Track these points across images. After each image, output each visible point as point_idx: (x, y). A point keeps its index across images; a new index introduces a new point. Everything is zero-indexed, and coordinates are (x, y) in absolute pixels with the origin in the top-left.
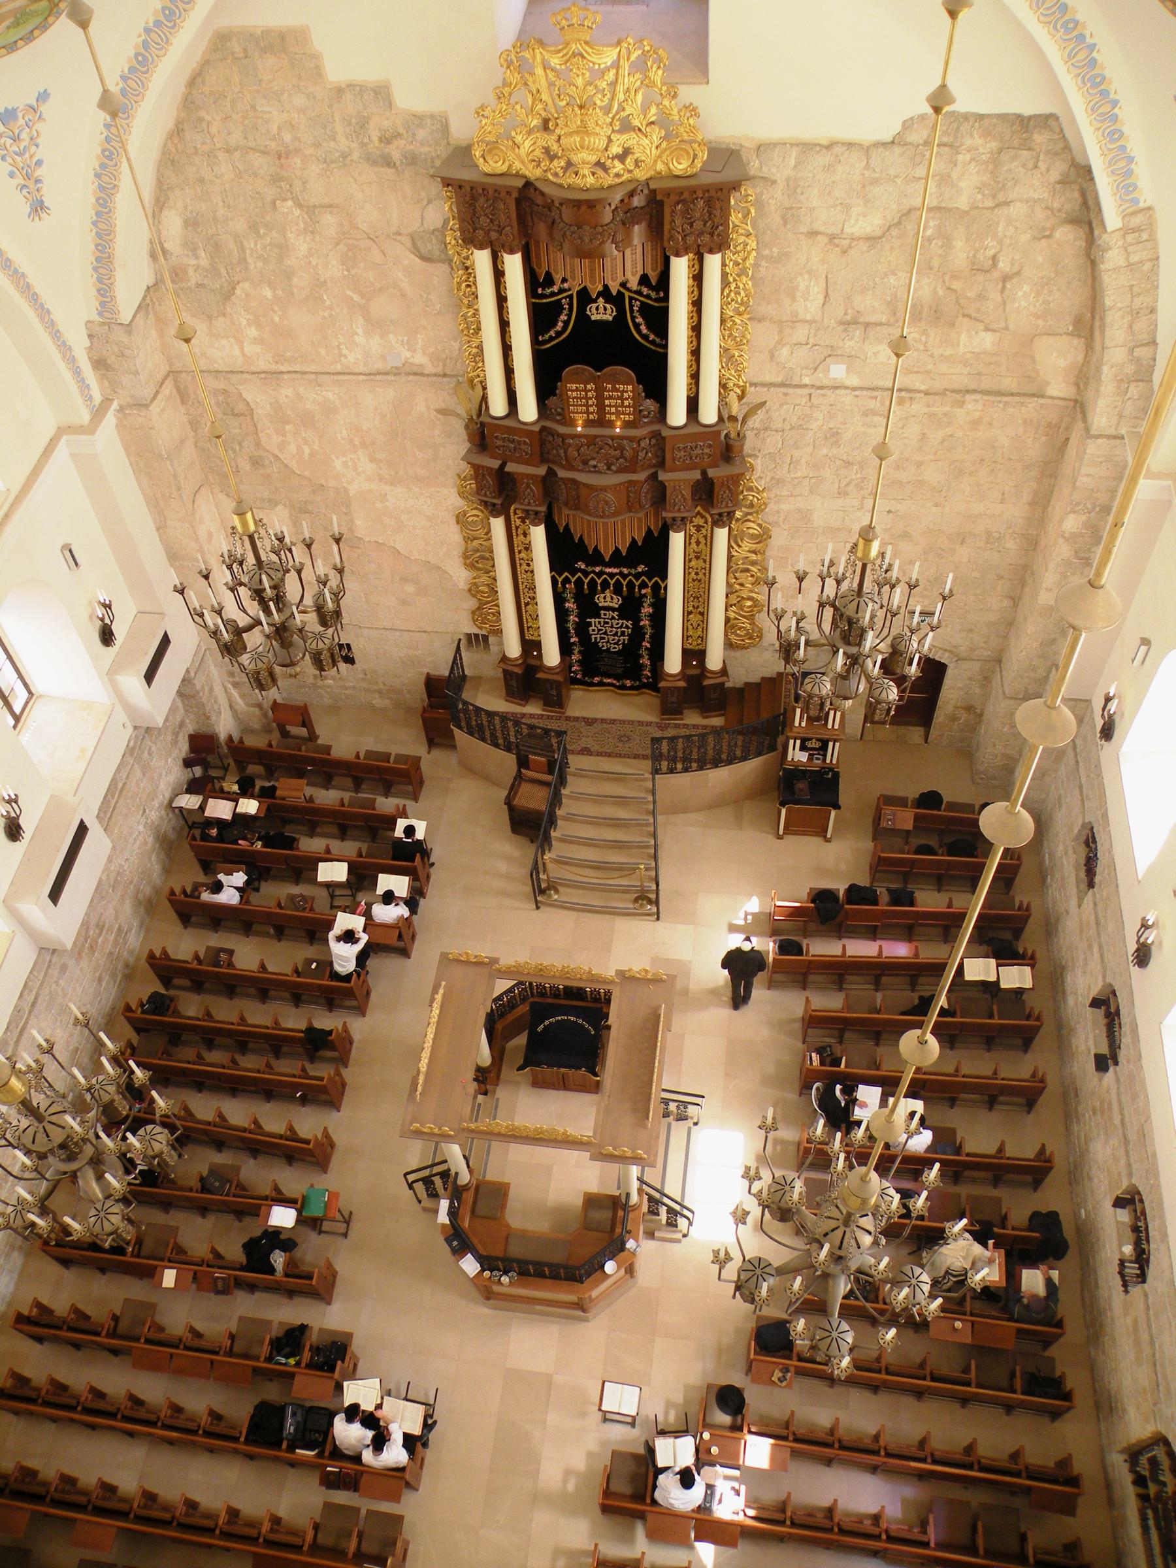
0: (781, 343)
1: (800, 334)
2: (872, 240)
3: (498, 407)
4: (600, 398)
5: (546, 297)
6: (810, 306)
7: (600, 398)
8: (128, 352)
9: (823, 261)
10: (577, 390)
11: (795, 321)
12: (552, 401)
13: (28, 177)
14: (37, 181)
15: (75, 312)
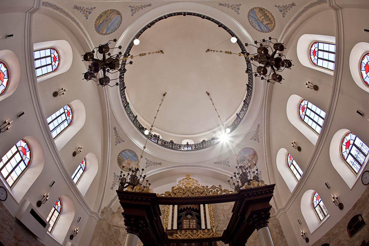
0: (218, 224)
1: (221, 222)
2: (228, 210)
3: (169, 228)
4: (189, 223)
5: (180, 215)
6: (222, 218)
7: (189, 223)
8: (108, 211)
9: (222, 212)
10: (185, 221)
11: (220, 220)
12: (180, 226)
13: (114, 184)
14: (114, 186)
15: (105, 204)
